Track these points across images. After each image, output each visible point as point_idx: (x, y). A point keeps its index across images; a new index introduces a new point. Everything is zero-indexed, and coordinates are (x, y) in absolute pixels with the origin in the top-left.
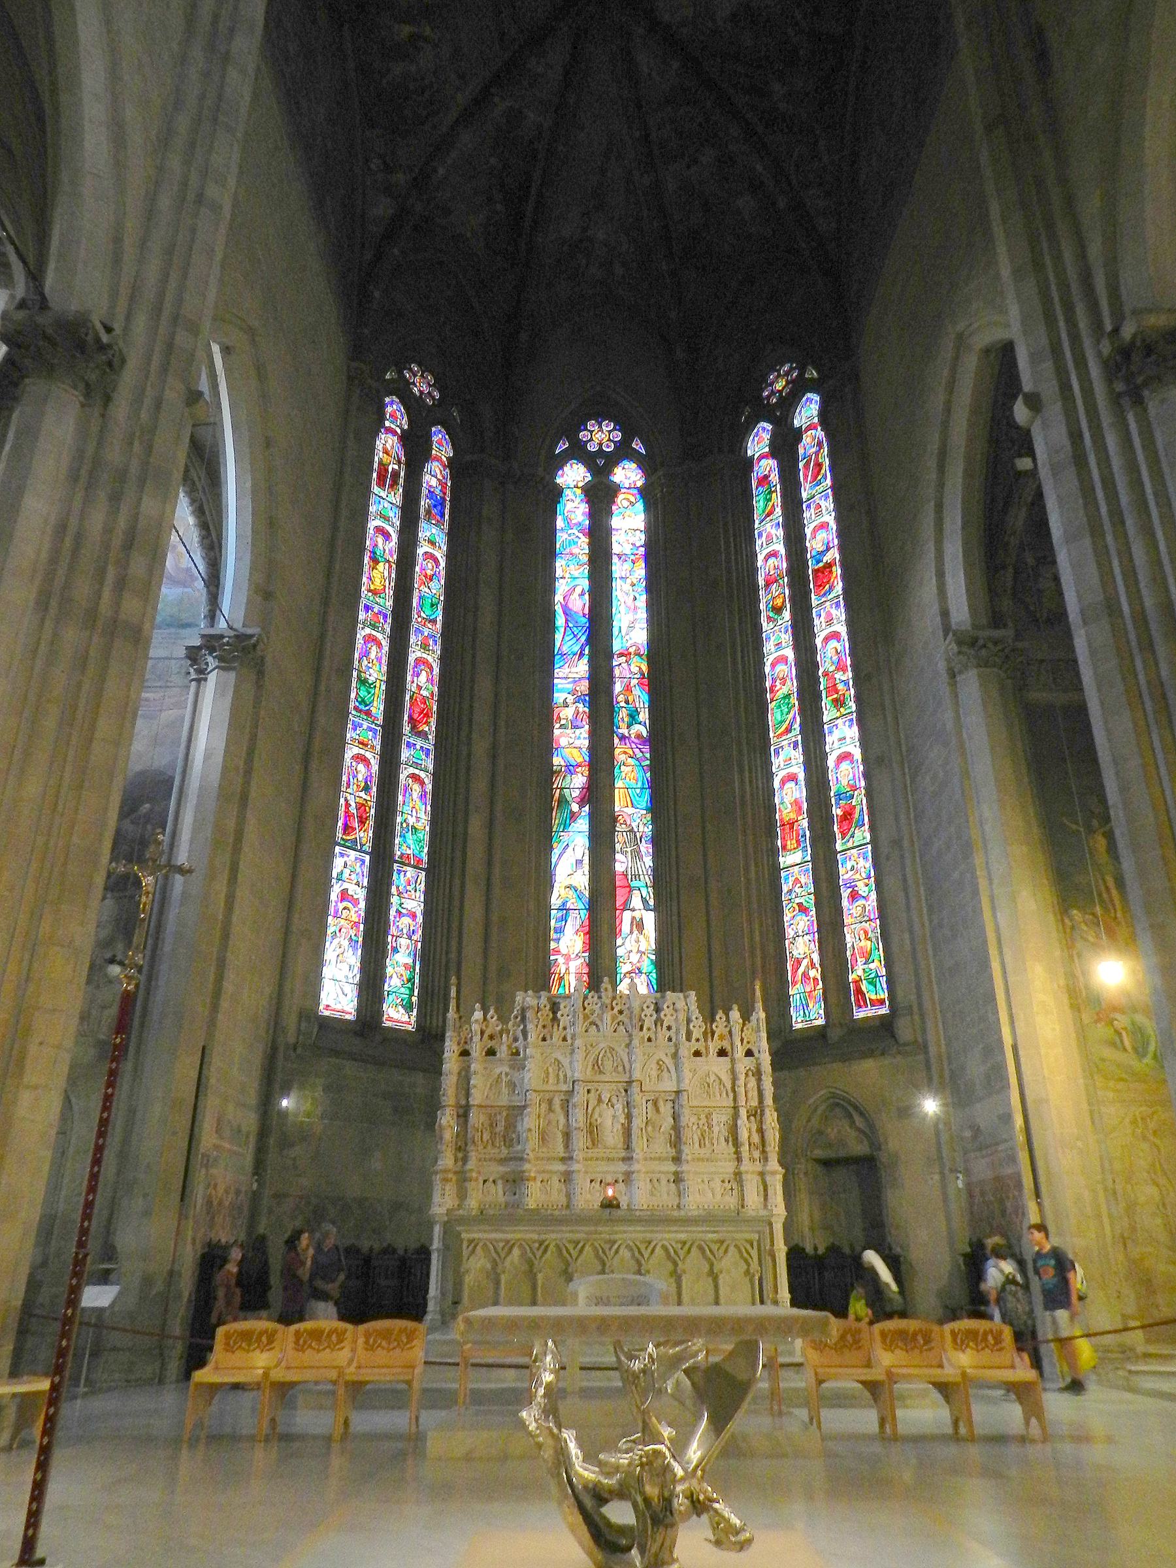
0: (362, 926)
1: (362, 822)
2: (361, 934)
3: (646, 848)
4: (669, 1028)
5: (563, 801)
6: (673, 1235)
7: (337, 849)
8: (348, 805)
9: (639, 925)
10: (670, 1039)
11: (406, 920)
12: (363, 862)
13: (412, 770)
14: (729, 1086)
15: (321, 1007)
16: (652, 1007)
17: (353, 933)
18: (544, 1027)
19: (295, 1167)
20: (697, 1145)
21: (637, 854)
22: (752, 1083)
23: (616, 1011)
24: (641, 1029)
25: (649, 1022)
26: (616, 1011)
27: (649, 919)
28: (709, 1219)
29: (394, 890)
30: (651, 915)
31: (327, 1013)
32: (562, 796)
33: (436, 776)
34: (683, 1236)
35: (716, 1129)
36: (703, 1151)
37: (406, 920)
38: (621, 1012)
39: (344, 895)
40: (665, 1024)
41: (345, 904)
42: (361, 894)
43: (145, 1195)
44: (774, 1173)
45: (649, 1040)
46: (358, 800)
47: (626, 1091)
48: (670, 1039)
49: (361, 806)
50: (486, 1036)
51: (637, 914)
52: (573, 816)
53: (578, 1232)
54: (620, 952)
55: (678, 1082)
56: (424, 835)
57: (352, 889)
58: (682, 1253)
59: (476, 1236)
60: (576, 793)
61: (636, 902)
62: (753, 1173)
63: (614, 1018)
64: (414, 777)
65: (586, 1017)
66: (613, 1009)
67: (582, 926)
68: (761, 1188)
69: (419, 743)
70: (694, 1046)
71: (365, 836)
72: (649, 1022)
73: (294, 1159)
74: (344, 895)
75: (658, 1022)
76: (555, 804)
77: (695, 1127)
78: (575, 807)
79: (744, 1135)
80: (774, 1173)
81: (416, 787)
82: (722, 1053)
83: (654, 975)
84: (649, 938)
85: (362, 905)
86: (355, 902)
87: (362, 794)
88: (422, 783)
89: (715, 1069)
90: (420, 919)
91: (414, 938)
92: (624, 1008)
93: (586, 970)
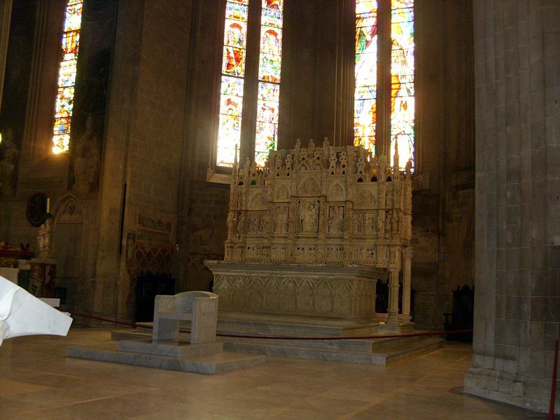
0: (240, 119)
1: (238, 60)
2: (240, 123)
3: (411, 60)
4: (344, 166)
5: (362, 34)
6: (312, 276)
7: (223, 78)
8: (229, 53)
9: (405, 106)
10: (344, 173)
11: (268, 114)
12: (240, 84)
13: (268, 28)
14: (376, 197)
15: (218, 161)
16: (335, 155)
17: (236, 122)
18: (278, 168)
19: (201, 241)
20: (356, 231)
21: (404, 62)
22: (390, 196)
23: (315, 158)
24: (328, 167)
25: (333, 163)
26: (315, 158)
27: (411, 102)
28: (329, 267)
29: (259, 97)
30: (413, 99)
31: (221, 165)
32: (361, 32)
33: (284, 29)
34: (317, 277)
35: (367, 222)
36: (360, 233)
37: (268, 114)
38: (318, 158)
39: (229, 102)
40: (342, 164)
41: (230, 106)
42: (239, 101)
43: (103, 251)
44: (395, 245)
45: (333, 173)
46: (235, 49)
47: (319, 202)
48: (344, 173)
49: (236, 53)
50: (251, 174)
51: (404, 100)
52: (368, 43)
53: (265, 273)
54: (392, 122)
55: (347, 196)
56: (278, 65)
57: (234, 99)
58: (316, 285)
59: (219, 273)
60: (369, 29)
61: (403, 92)
62: (383, 245)
63: (314, 161)
64: (271, 32)
65: (299, 162)
66: (314, 157)
67: (372, 108)
68: (388, 254)
69: (273, 11)
70: (358, 176)
71: (240, 69)
72: (333, 163)
73: (200, 237)
74: (229, 102)
75: (338, 163)
76: (357, 37)
77: (356, 221)
78: (368, 37)
79: (381, 225)
80: (395, 245)
81: (272, 37)
82: (374, 179)
83: (413, 136)
84: (410, 114)
85: (240, 107)
86: (236, 105)
87: (238, 46)
88: (276, 34)
89: (369, 188)
90: (277, 111)
91: (274, 122)
92: (320, 156)
93: (374, 134)
